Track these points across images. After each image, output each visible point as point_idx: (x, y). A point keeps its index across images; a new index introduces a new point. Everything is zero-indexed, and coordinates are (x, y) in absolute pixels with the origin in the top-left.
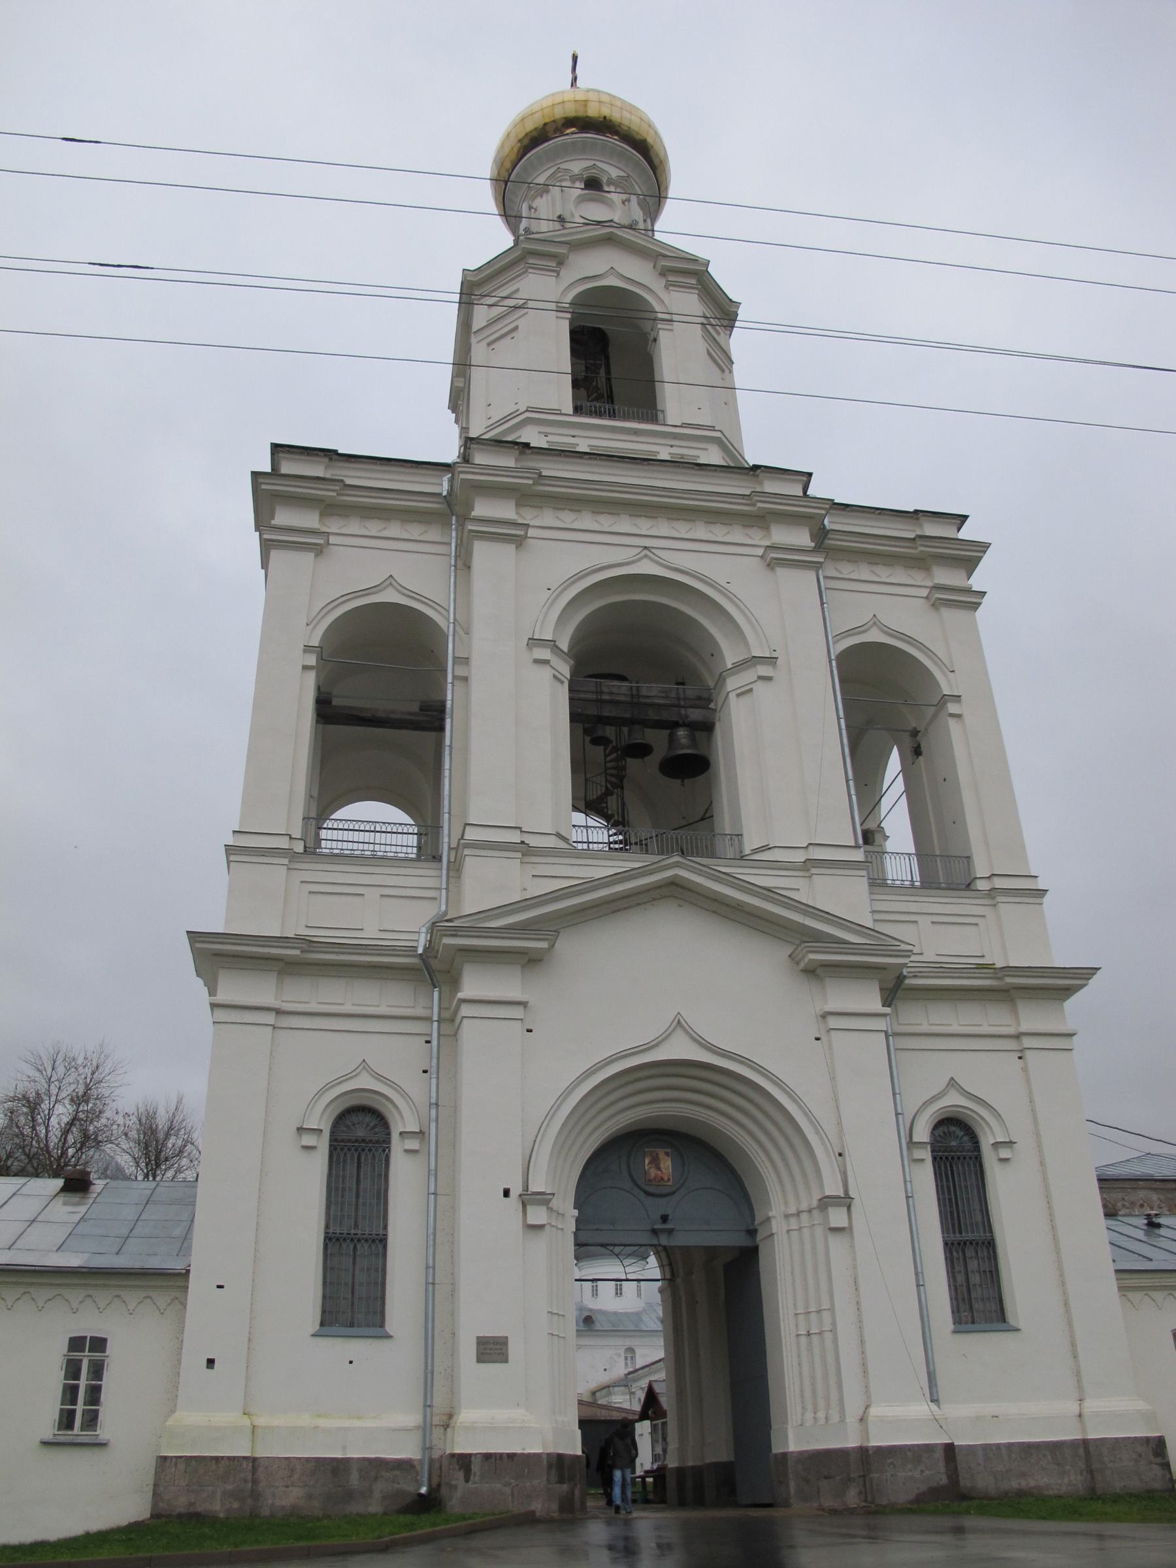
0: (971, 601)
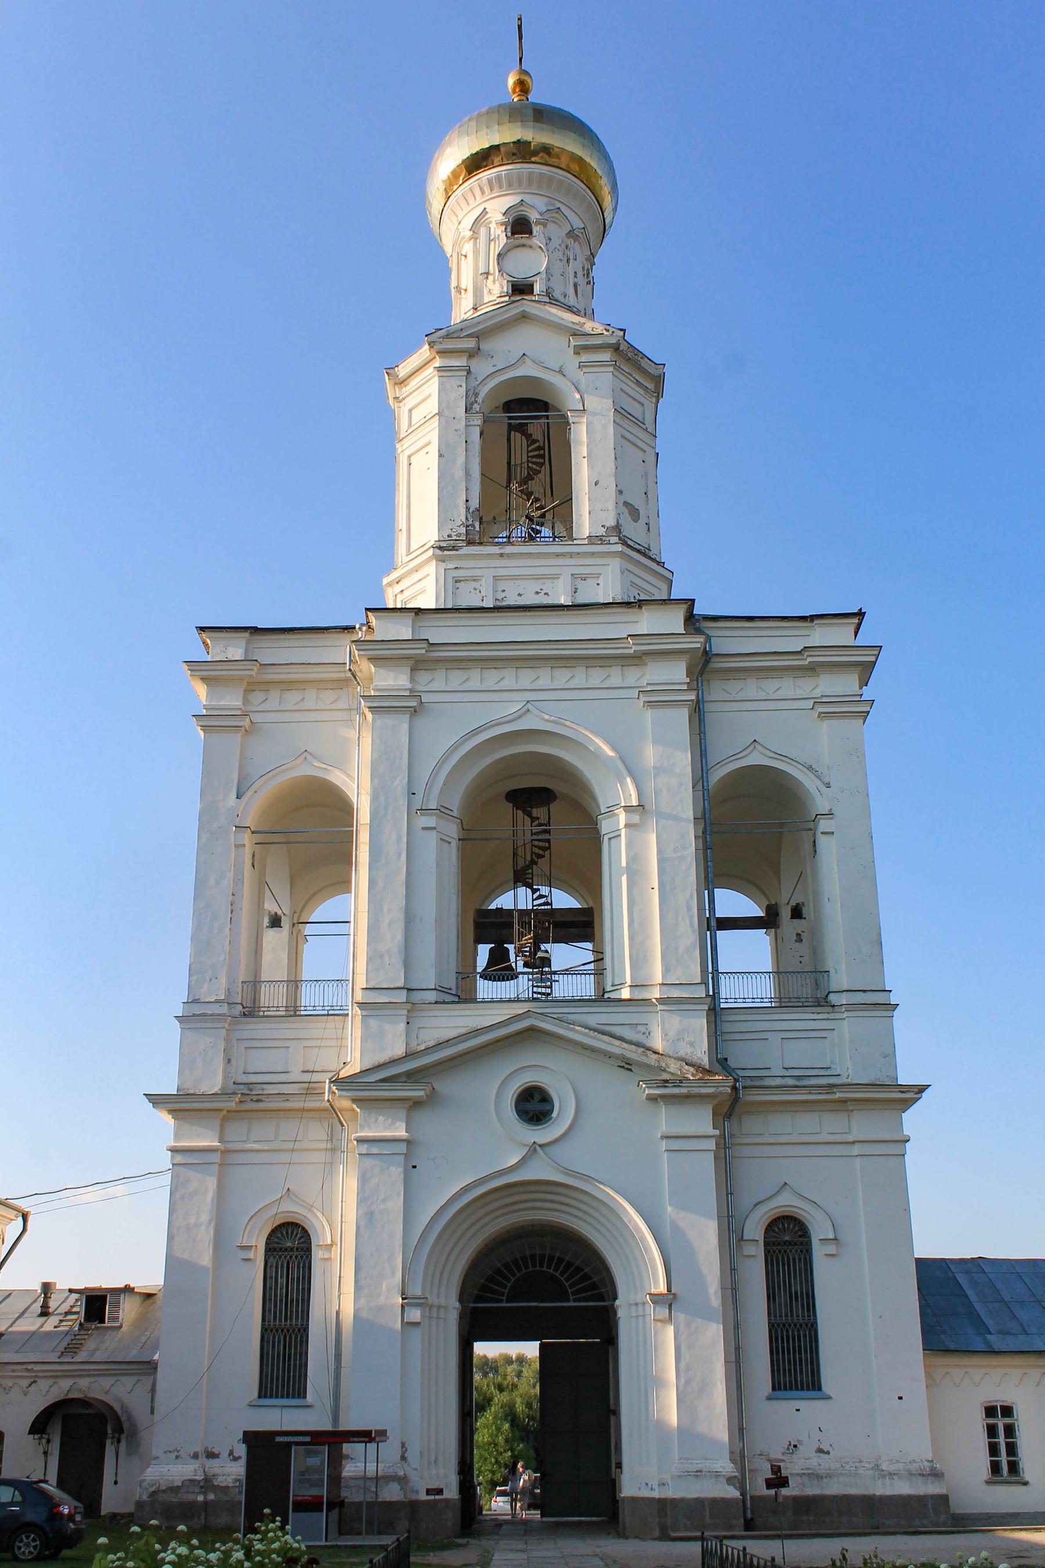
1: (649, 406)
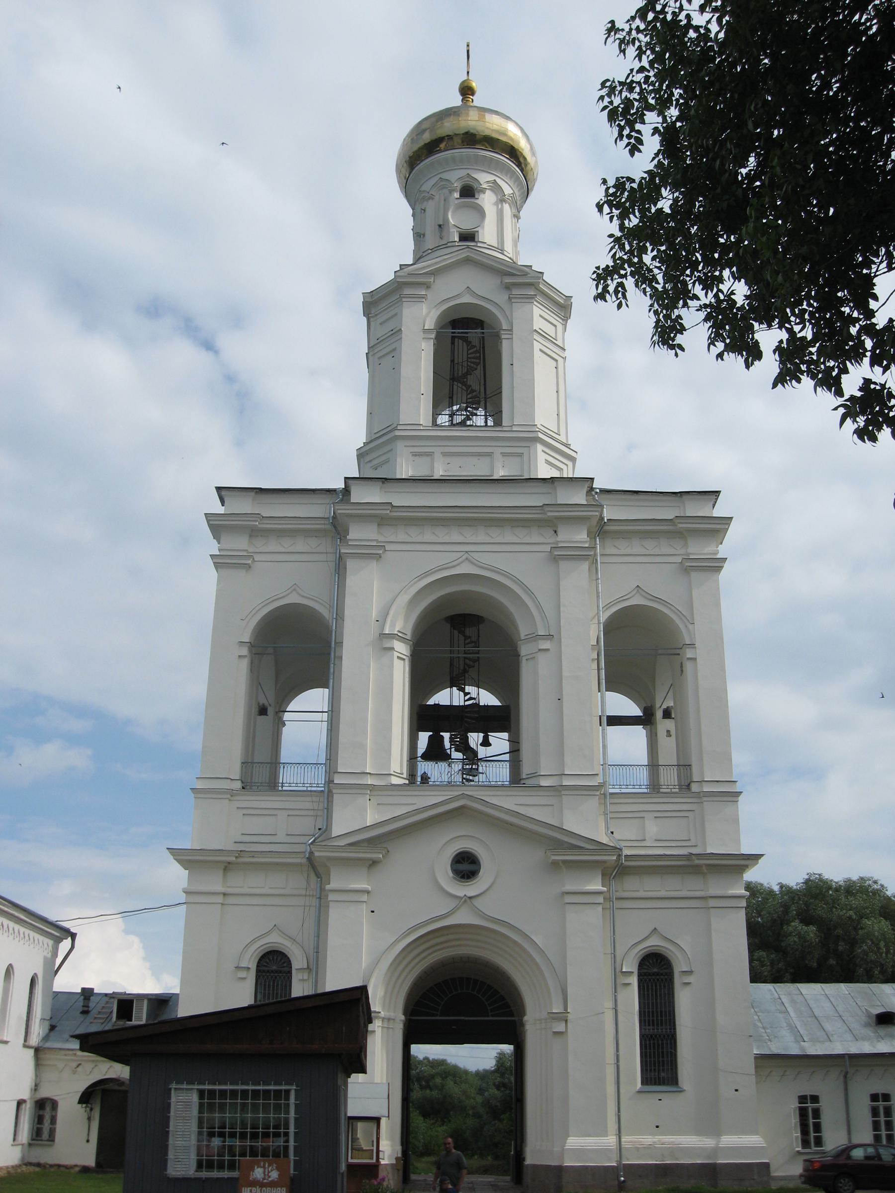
0: (715, 565)
1: (560, 327)
